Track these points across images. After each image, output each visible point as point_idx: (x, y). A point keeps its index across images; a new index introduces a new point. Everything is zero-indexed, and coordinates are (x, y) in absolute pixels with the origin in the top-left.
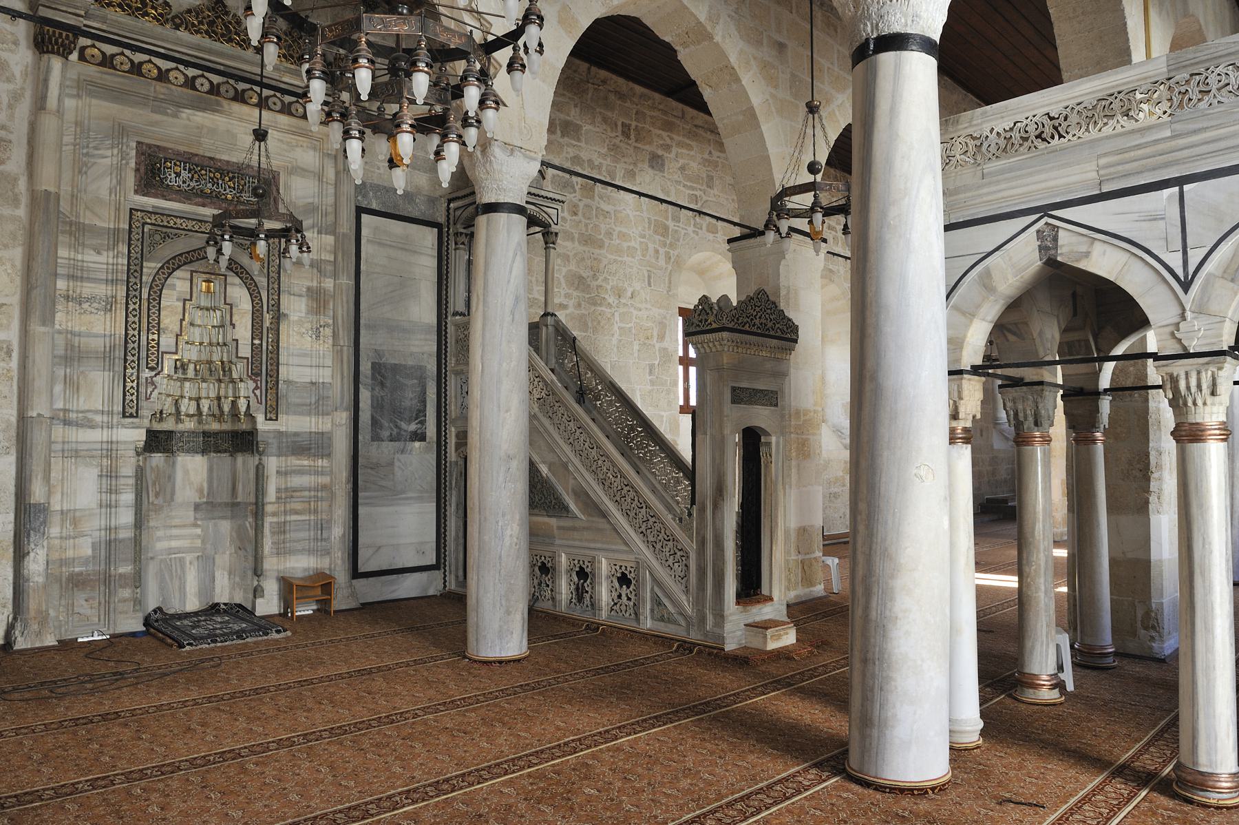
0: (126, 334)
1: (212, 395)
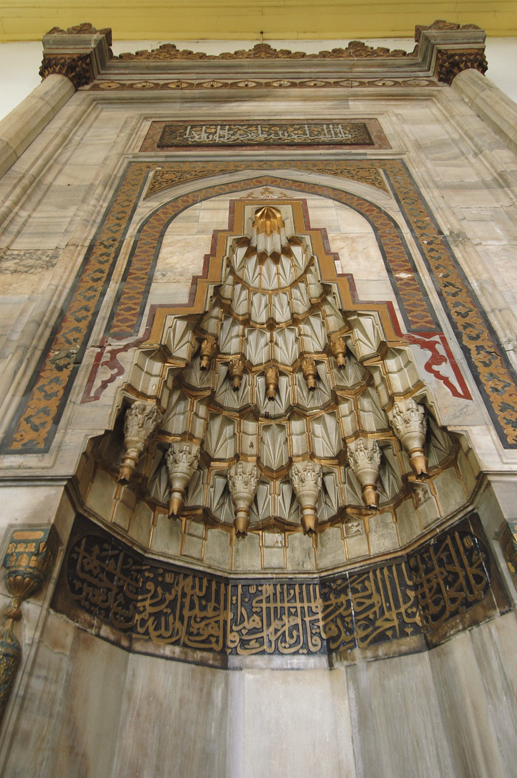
0: (74, 289)
1: (325, 446)
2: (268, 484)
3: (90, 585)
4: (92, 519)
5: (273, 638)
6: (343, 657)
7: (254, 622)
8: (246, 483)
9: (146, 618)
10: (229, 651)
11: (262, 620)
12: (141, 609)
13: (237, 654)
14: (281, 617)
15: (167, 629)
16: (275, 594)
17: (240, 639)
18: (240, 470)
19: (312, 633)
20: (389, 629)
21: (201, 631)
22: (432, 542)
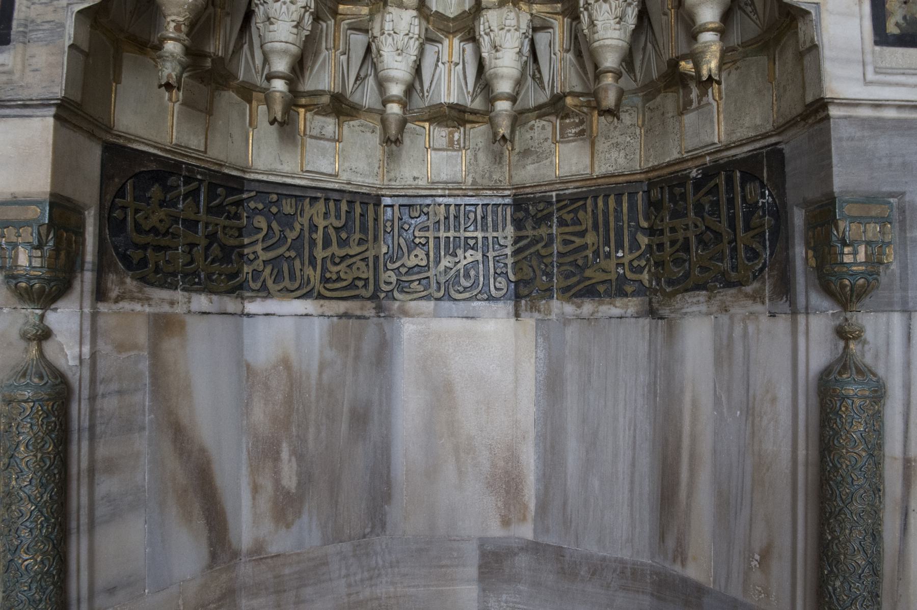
2: (441, 43)
3: (158, 248)
4: (135, 146)
5: (442, 280)
6: (533, 308)
7: (417, 258)
8: (400, 52)
9: (261, 268)
10: (382, 295)
11: (427, 255)
12: (252, 257)
13: (395, 299)
14: (455, 249)
15: (292, 277)
16: (447, 218)
17: (397, 280)
18: (388, 26)
19: (495, 273)
20: (603, 282)
21: (342, 275)
22: (694, 173)
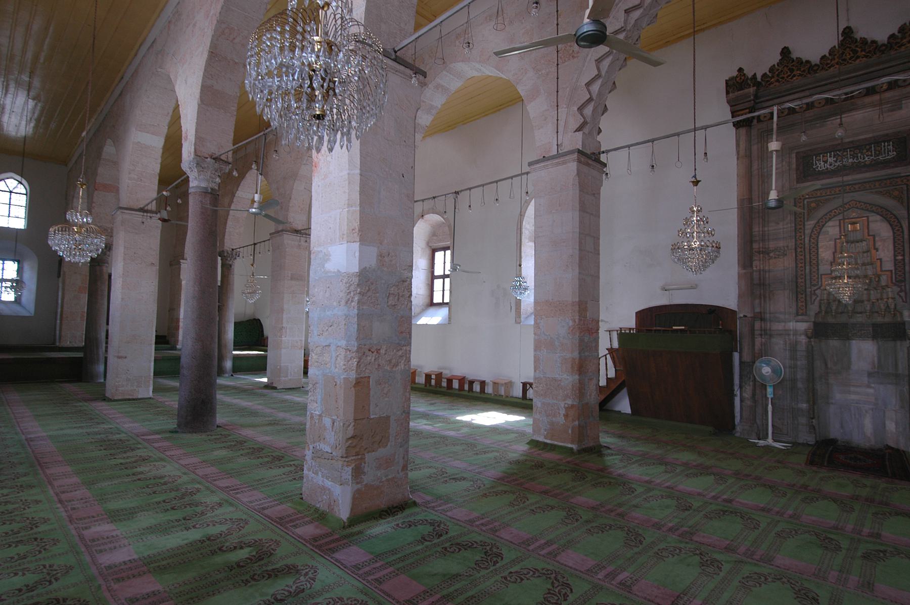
0: (796, 267)
